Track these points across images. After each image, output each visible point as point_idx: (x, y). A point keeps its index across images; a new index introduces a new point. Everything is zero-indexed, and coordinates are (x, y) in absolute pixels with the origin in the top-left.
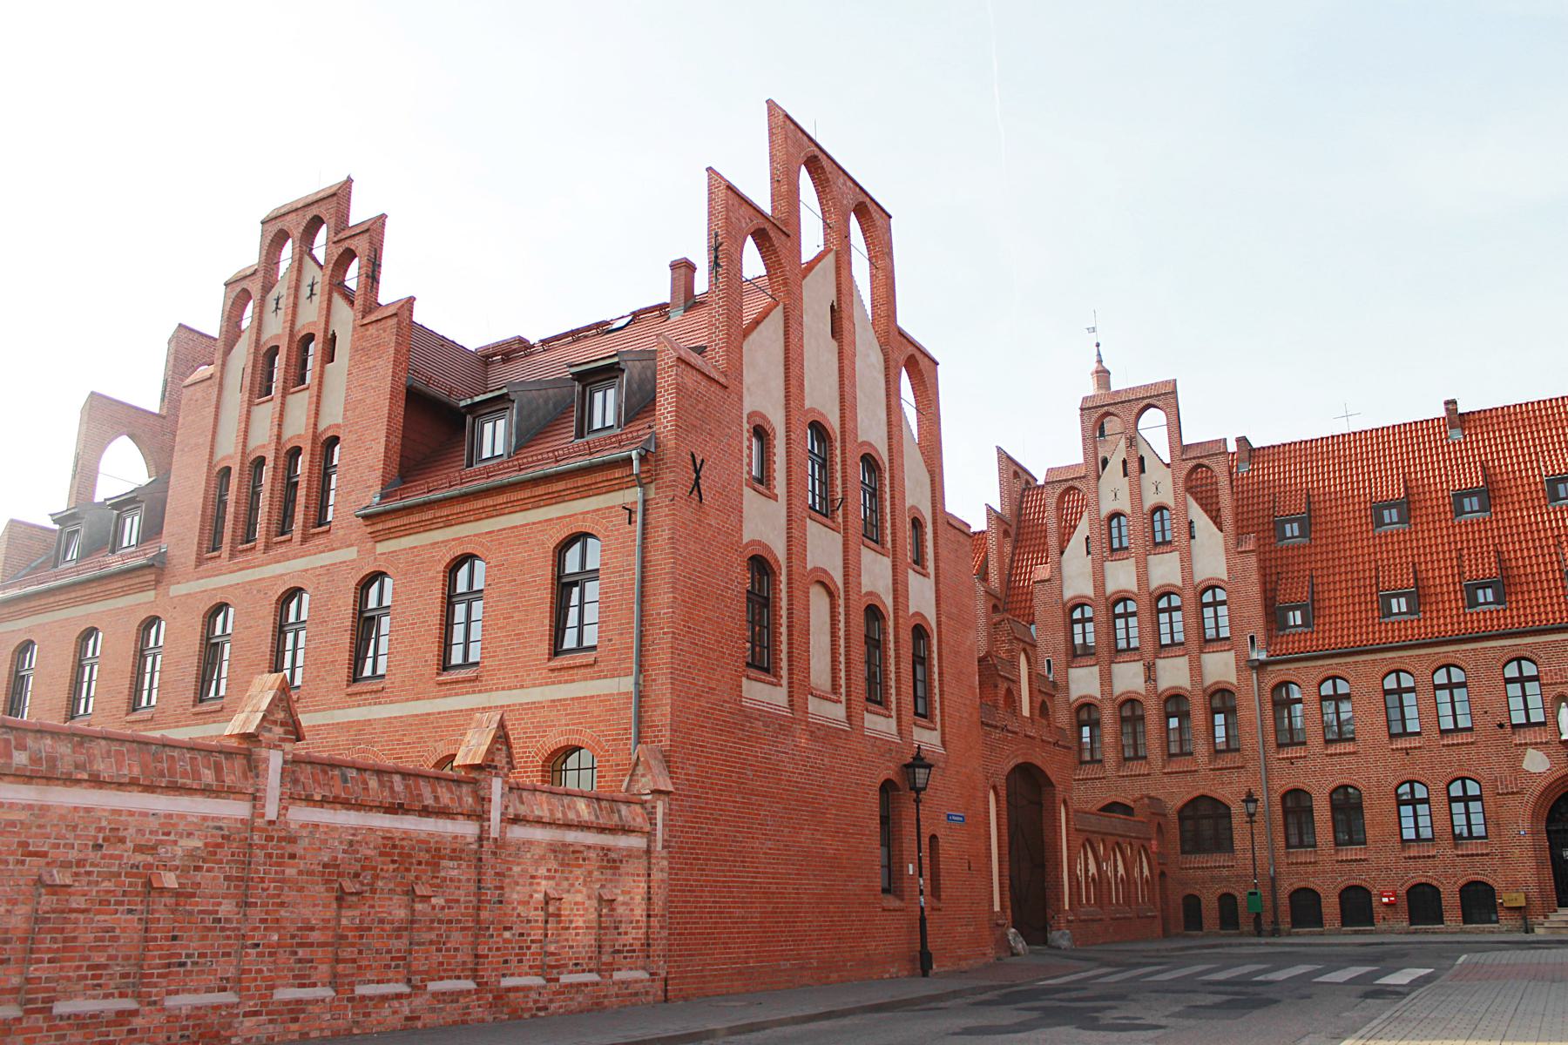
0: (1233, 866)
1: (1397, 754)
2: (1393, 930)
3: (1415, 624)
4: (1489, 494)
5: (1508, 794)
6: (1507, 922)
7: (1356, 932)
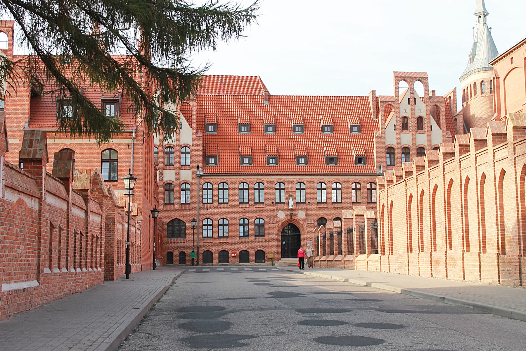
2: (234, 264)
3: (251, 168)
4: (275, 127)
6: (267, 262)
7: (223, 265)
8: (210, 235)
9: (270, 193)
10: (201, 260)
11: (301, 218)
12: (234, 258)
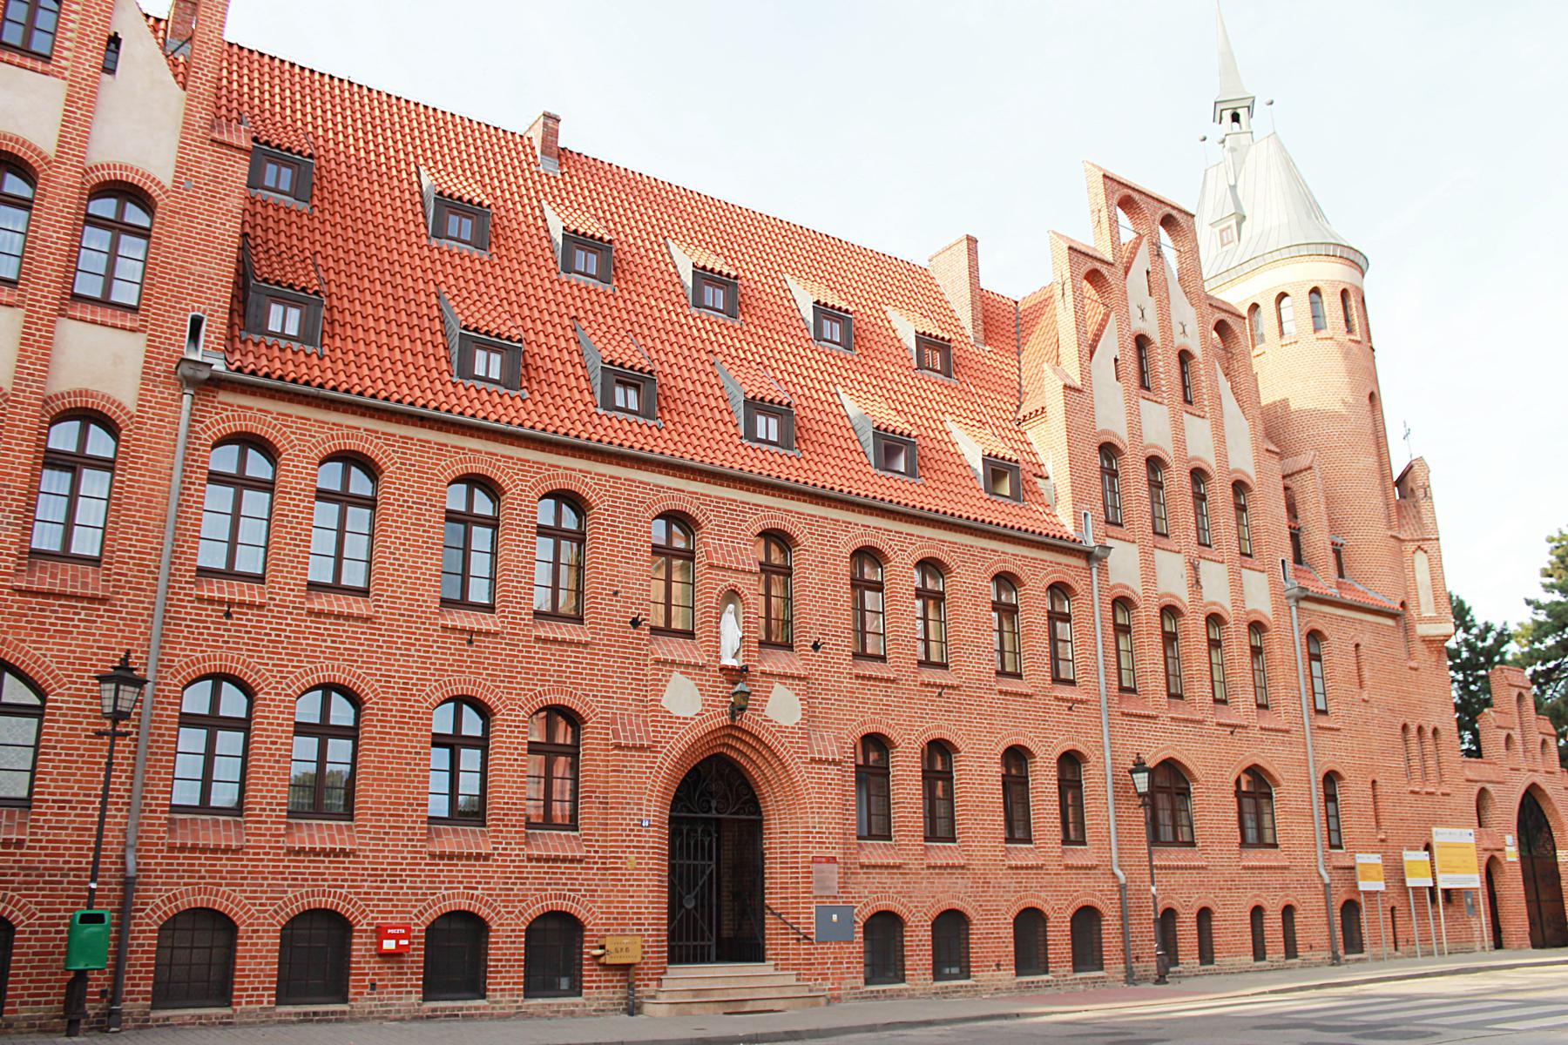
0: (20, 844)
1: (452, 638)
5: (634, 748)
6: (599, 992)
8: (224, 795)
9: (623, 567)
10: (138, 986)
11: (781, 729)
12: (387, 969)
